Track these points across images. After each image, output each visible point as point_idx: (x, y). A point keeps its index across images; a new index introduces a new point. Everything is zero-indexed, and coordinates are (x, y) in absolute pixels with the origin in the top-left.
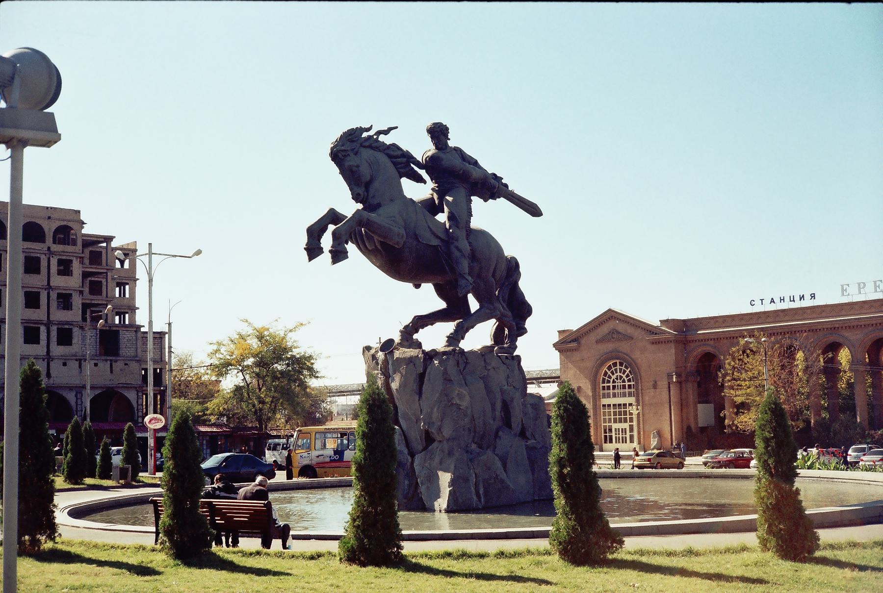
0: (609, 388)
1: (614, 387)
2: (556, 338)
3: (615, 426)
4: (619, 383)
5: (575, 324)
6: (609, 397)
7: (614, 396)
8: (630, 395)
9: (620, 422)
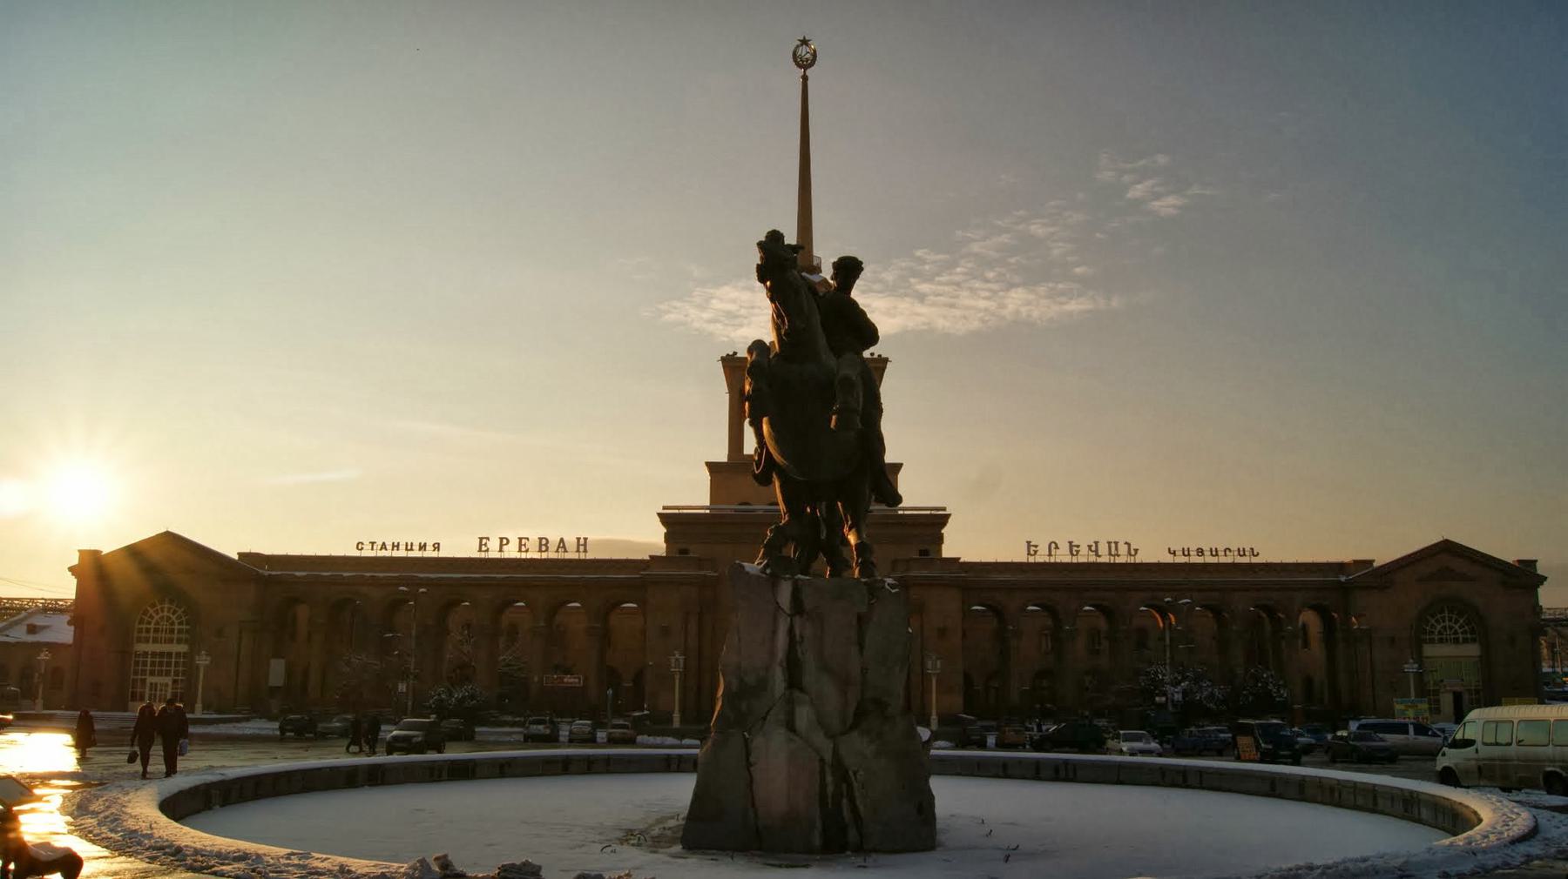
0: (148, 631)
1: (156, 630)
2: (75, 561)
3: (150, 679)
4: (165, 625)
5: (109, 543)
6: (147, 641)
7: (155, 641)
8: (179, 641)
9: (160, 674)
